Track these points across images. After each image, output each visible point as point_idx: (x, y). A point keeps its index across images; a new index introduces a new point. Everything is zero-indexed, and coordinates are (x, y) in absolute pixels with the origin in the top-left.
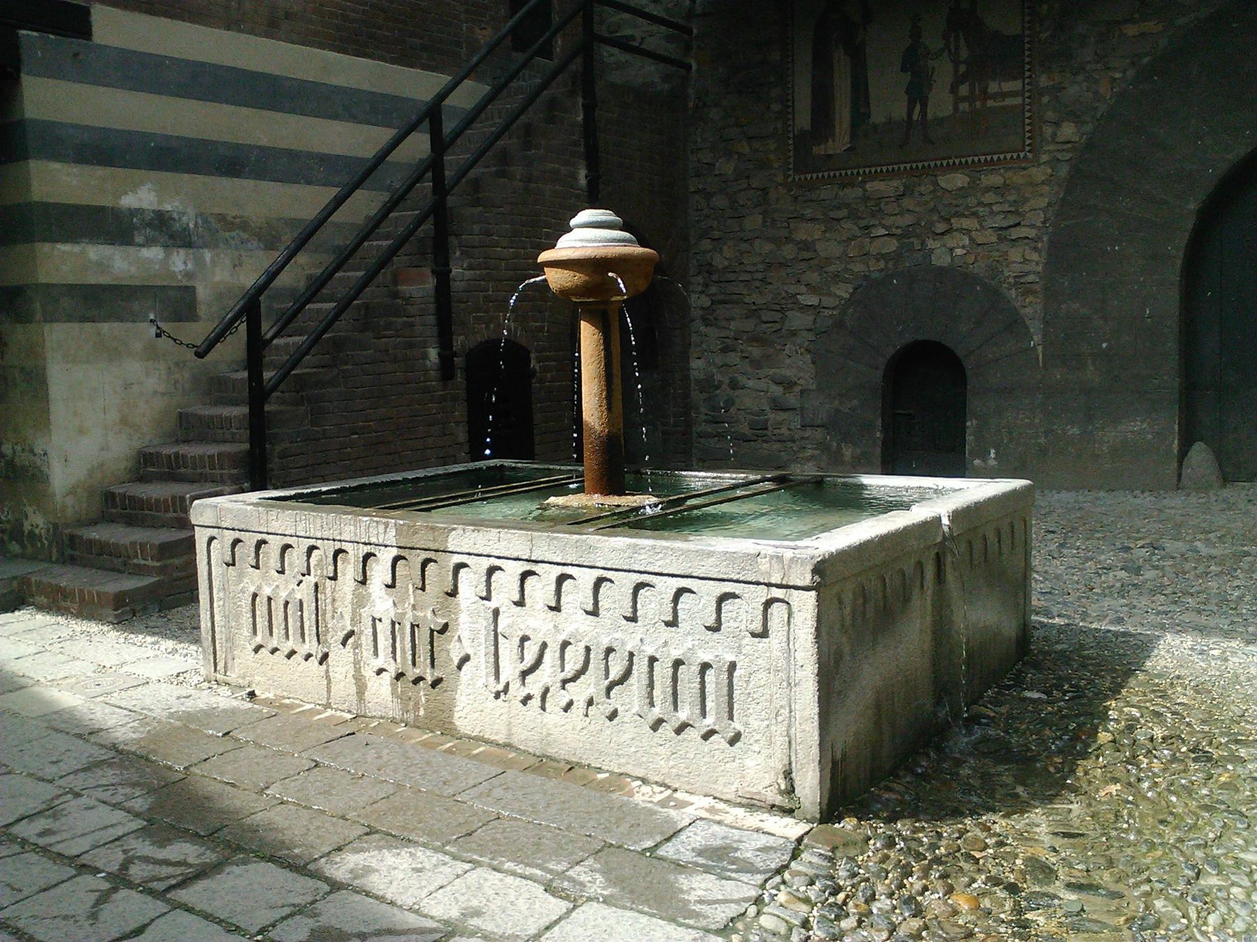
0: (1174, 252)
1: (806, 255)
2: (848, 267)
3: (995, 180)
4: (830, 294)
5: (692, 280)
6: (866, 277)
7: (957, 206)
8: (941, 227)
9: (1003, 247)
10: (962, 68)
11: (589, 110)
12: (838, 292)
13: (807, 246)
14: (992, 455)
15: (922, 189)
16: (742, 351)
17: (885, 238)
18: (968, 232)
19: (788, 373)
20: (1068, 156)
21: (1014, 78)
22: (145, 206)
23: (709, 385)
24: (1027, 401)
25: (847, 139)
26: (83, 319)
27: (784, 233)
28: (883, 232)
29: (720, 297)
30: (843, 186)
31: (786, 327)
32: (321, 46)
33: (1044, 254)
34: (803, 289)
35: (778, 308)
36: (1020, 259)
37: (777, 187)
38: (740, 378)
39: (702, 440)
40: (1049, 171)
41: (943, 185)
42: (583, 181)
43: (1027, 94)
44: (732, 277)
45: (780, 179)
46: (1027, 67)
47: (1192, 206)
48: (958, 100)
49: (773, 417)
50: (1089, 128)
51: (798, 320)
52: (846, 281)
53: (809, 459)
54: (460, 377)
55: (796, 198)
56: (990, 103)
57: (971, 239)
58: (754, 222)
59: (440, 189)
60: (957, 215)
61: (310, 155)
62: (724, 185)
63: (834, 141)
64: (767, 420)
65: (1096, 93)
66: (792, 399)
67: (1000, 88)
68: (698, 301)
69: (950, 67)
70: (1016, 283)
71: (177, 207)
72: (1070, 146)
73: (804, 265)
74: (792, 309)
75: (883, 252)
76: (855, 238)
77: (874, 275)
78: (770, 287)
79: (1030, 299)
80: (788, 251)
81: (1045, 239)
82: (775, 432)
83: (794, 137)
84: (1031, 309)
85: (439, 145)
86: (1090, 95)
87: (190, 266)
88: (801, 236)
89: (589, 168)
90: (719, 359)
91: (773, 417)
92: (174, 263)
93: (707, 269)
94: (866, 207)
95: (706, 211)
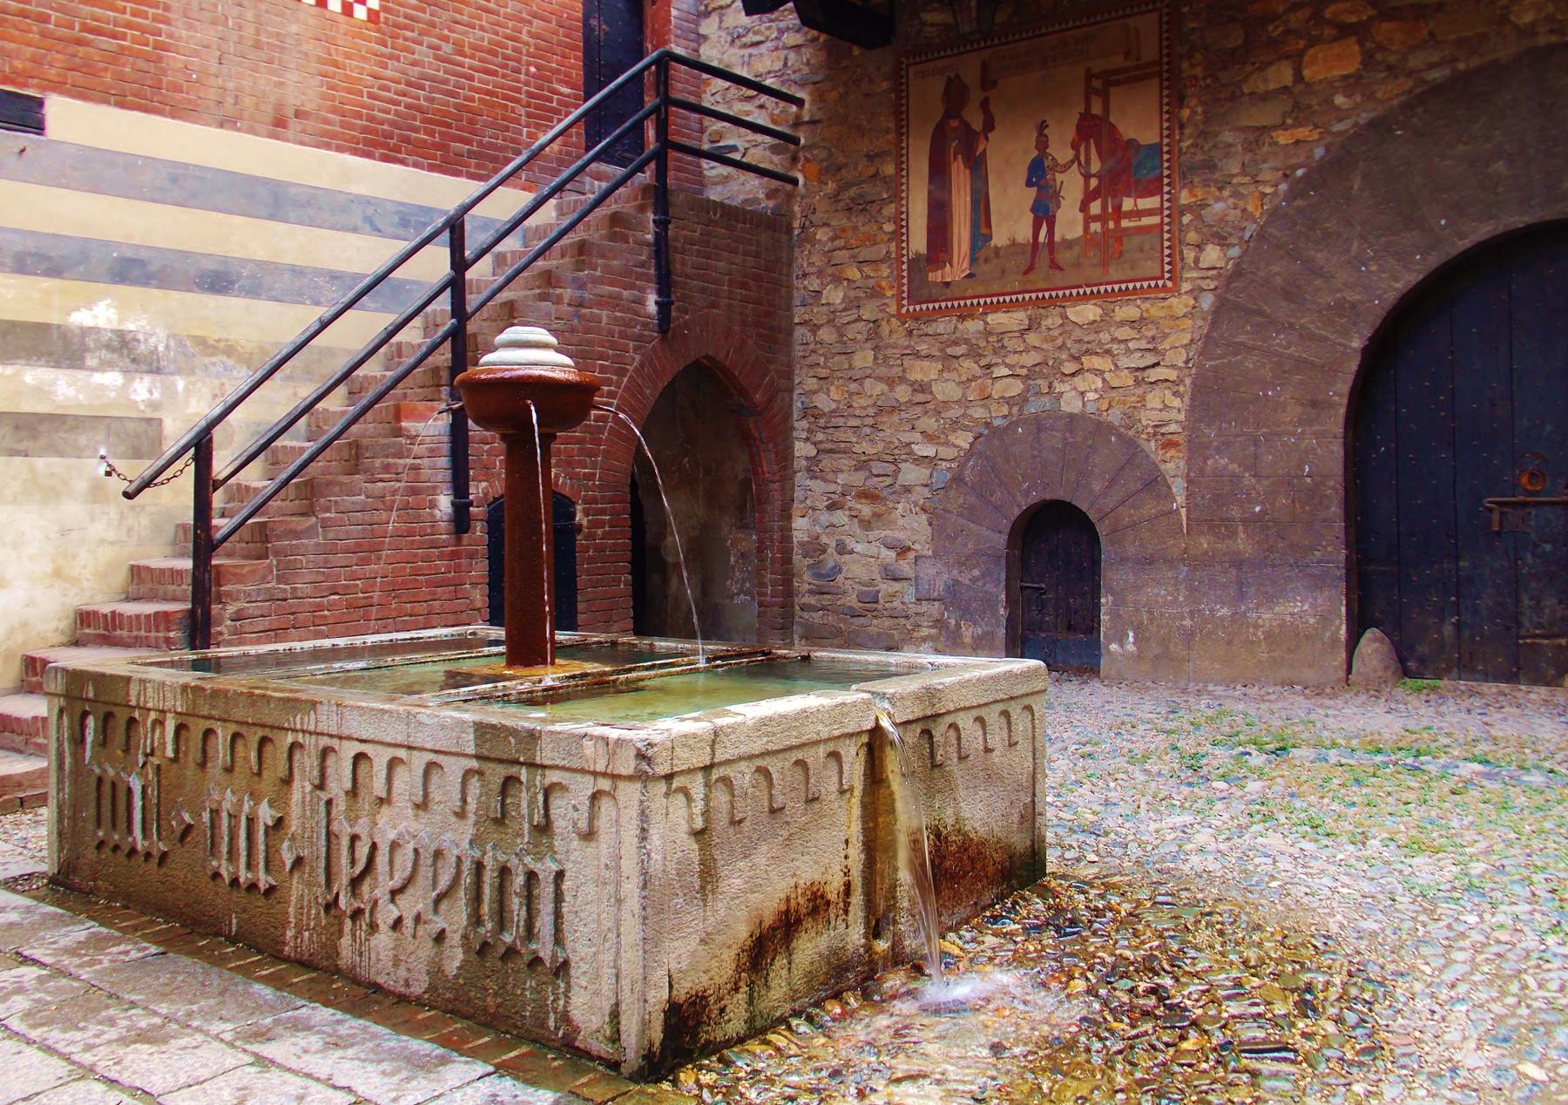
0: (1336, 398)
1: (921, 397)
2: (970, 412)
4: (947, 444)
5: (796, 425)
6: (987, 425)
7: (1089, 343)
8: (1069, 368)
9: (1139, 391)
10: (1094, 182)
11: (662, 224)
12: (957, 442)
13: (922, 387)
14: (1131, 639)
16: (850, 509)
17: (1010, 380)
18: (1099, 372)
19: (901, 535)
21: (1152, 194)
22: (102, 323)
23: (815, 548)
24: (1170, 574)
25: (966, 265)
26: (13, 453)
27: (897, 371)
28: (1006, 371)
29: (829, 446)
30: (962, 318)
31: (899, 482)
32: (339, 149)
33: (1187, 399)
34: (917, 436)
35: (890, 458)
37: (888, 321)
38: (847, 541)
39: (805, 615)
40: (1192, 302)
41: (1073, 318)
42: (652, 308)
43: (1166, 212)
44: (841, 421)
45: (892, 309)
46: (1166, 181)
47: (1357, 344)
48: (1088, 219)
49: (886, 588)
50: (1235, 252)
51: (911, 474)
52: (966, 428)
53: (924, 639)
54: (479, 530)
55: (911, 331)
56: (1125, 223)
57: (1104, 380)
58: (864, 358)
59: (459, 310)
60: (1087, 352)
61: (318, 272)
62: (832, 316)
63: (951, 266)
64: (878, 592)
65: (1244, 210)
66: (905, 567)
67: (1136, 205)
68: (802, 449)
69: (1081, 180)
70: (1155, 434)
71: (143, 327)
72: (1214, 272)
73: (919, 409)
74: (906, 461)
75: (1007, 395)
76: (975, 378)
77: (997, 422)
78: (881, 434)
79: (1173, 452)
80: (902, 393)
81: (1188, 381)
82: (887, 605)
83: (909, 260)
84: (1173, 466)
85: (460, 264)
87: (156, 395)
88: (915, 375)
89: (660, 293)
90: (825, 518)
91: (886, 588)
92: (135, 391)
93: (811, 412)
94: (988, 342)
95: (812, 346)
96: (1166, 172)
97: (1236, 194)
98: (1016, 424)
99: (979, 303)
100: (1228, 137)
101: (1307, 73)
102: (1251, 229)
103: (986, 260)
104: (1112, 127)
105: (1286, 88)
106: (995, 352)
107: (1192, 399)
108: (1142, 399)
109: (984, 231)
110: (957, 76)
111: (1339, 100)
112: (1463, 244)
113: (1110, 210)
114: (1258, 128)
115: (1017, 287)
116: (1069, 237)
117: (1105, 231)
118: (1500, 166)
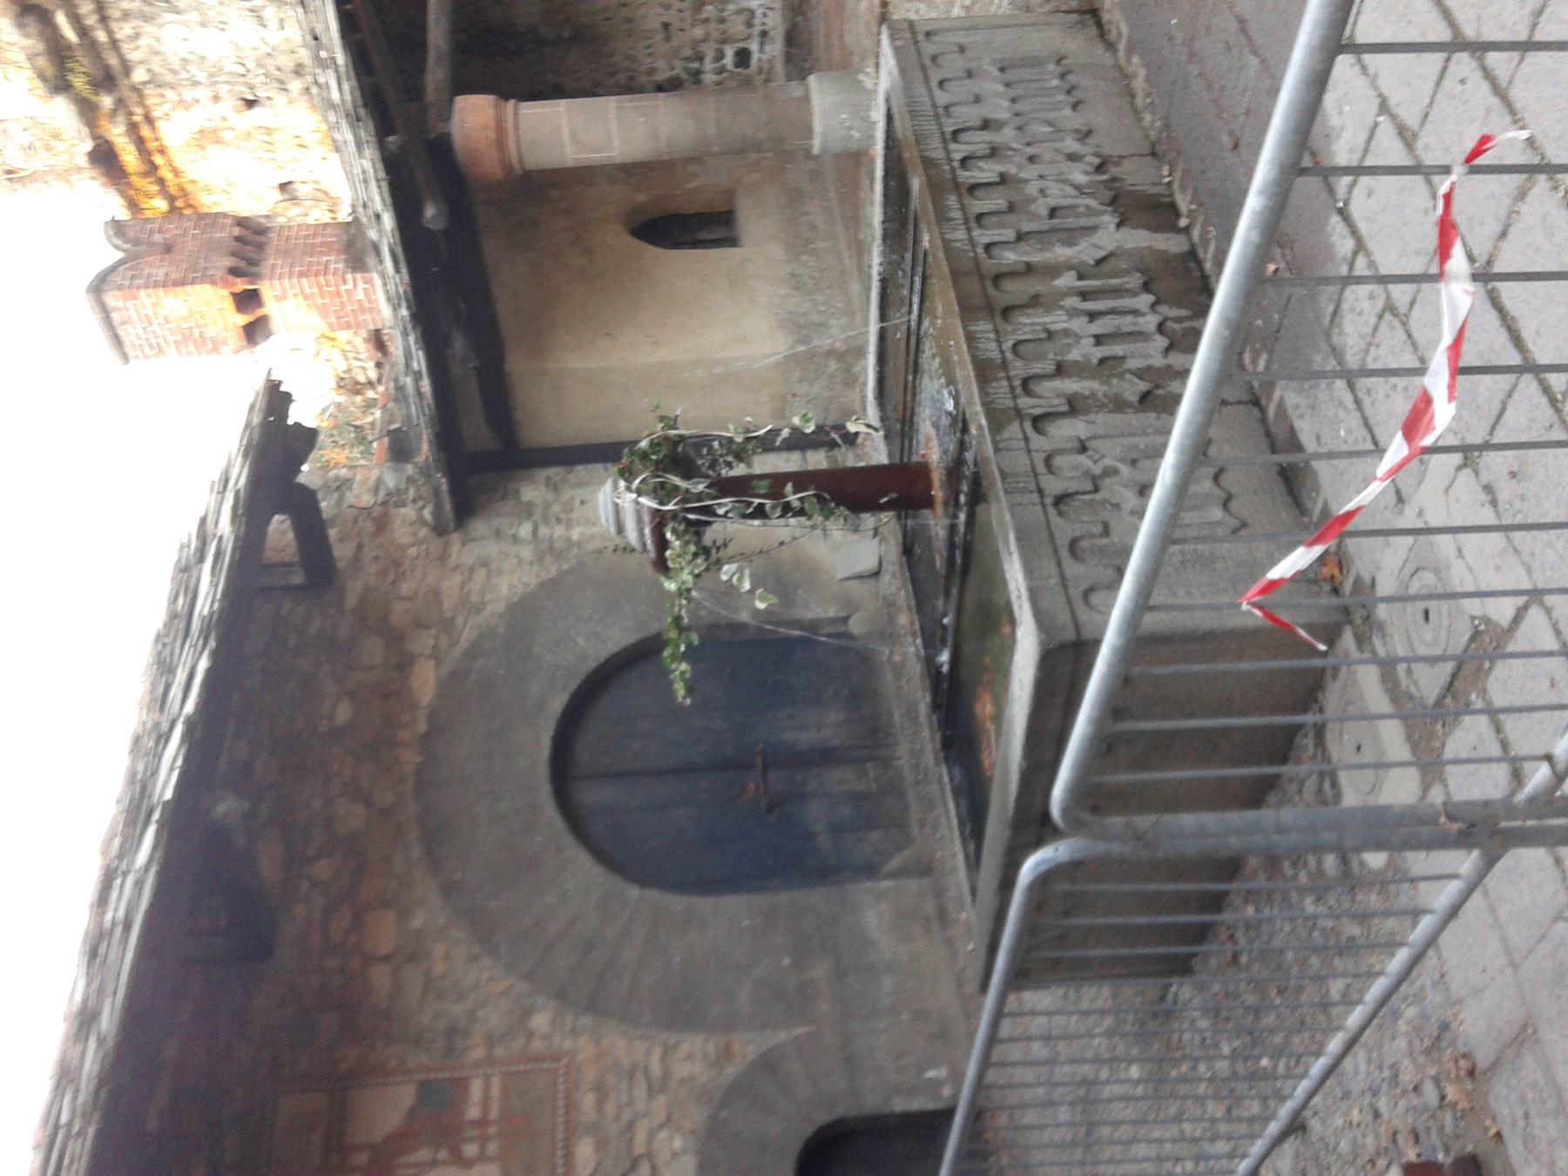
10: (443, 1154)
18: (652, 1133)
47: (634, 892)
48: (482, 1158)
50: (541, 1000)
56: (494, 1114)
57: (662, 1126)
60: (631, 1141)
79: (736, 1047)
84: (749, 1046)
101: (384, 950)
102: (522, 987)
104: (389, 1139)
108: (683, 1081)
111: (417, 922)
112: (559, 823)
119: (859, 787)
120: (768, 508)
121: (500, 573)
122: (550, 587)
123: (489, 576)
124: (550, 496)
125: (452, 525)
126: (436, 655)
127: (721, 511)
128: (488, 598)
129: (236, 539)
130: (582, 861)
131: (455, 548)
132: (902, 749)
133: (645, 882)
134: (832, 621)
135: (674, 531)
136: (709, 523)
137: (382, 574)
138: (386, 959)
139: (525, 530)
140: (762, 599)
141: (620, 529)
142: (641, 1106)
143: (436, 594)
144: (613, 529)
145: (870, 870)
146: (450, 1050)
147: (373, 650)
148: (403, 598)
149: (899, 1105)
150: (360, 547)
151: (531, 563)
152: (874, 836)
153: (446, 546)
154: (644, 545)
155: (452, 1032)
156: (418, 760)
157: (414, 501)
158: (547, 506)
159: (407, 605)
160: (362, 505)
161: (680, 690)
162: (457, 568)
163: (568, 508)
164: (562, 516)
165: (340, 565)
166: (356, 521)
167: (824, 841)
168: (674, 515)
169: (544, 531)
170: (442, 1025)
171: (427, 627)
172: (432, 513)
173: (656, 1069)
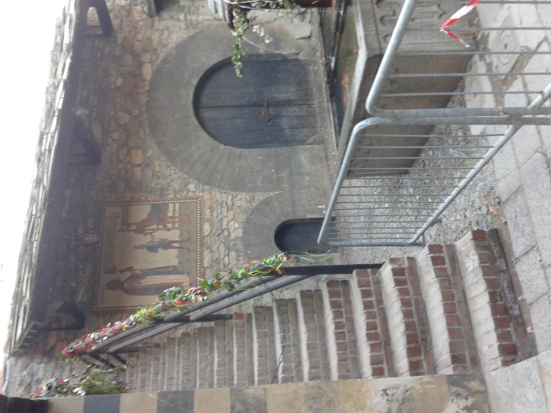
3: (208, 212)
9: (235, 208)
15: (209, 241)
20: (201, 186)
21: (168, 206)
25: (183, 276)
28: (226, 258)
33: (239, 193)
36: (240, 202)
40: (206, 192)
47: (222, 147)
48: (174, 228)
50: (191, 180)
56: (177, 215)
57: (231, 220)
63: (183, 283)
65: (179, 178)
69: (159, 232)
75: (235, 257)
79: (256, 197)
81: (232, 193)
84: (260, 197)
86: (179, 180)
94: (215, 266)
96: (162, 202)
97: (172, 181)
98: (246, 253)
99: (200, 270)
100: (153, 185)
101: (138, 163)
102: (185, 176)
103: (183, 267)
104: (142, 221)
105: (142, 170)
106: (219, 264)
107: (238, 191)
109: (171, 269)
110: (107, 284)
111: (149, 154)
112: (196, 123)
113: (171, 220)
114: (153, 176)
115: (195, 254)
116: (178, 235)
117: (179, 222)
118: (176, 116)
119: (300, 114)
120: (270, 4)
121: (173, 32)
122: (191, 38)
123: (169, 34)
124: (191, 4)
125: (155, 13)
126: (151, 62)
127: (253, 5)
128: (169, 42)
129: (77, 15)
130: (205, 135)
131: (156, 23)
132: (316, 102)
133: (225, 144)
134: (293, 54)
135: (236, 12)
136: (249, 10)
137: (130, 31)
138: (139, 165)
139: (182, 16)
140: (268, 39)
141: (216, 11)
142: (225, 214)
143: (150, 39)
144: (213, 11)
145: (303, 142)
146: (162, 195)
147: (128, 59)
148: (139, 41)
149: (309, 216)
150: (122, 21)
151: (184, 29)
152: (305, 130)
153: (153, 22)
154: (225, 18)
155: (162, 189)
156: (147, 99)
157: (141, 4)
158: (190, 7)
159: (139, 43)
160: (122, 5)
161: (238, 72)
162: (157, 30)
163: (198, 9)
164: (196, 12)
165: (115, 27)
166: (119, 11)
167: (287, 132)
168: (236, 6)
169: (189, 17)
170: (159, 187)
171: (148, 52)
172: (147, 9)
173: (230, 203)
